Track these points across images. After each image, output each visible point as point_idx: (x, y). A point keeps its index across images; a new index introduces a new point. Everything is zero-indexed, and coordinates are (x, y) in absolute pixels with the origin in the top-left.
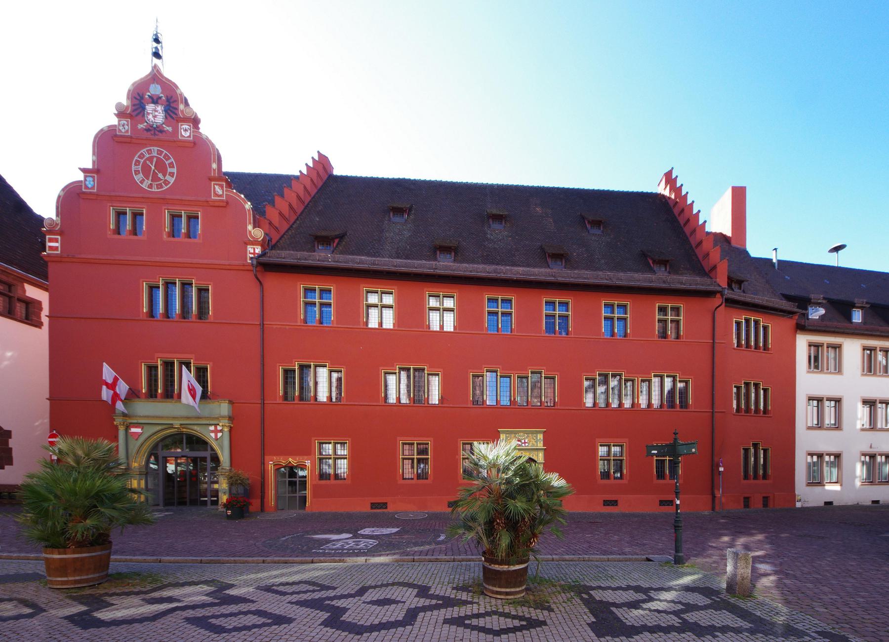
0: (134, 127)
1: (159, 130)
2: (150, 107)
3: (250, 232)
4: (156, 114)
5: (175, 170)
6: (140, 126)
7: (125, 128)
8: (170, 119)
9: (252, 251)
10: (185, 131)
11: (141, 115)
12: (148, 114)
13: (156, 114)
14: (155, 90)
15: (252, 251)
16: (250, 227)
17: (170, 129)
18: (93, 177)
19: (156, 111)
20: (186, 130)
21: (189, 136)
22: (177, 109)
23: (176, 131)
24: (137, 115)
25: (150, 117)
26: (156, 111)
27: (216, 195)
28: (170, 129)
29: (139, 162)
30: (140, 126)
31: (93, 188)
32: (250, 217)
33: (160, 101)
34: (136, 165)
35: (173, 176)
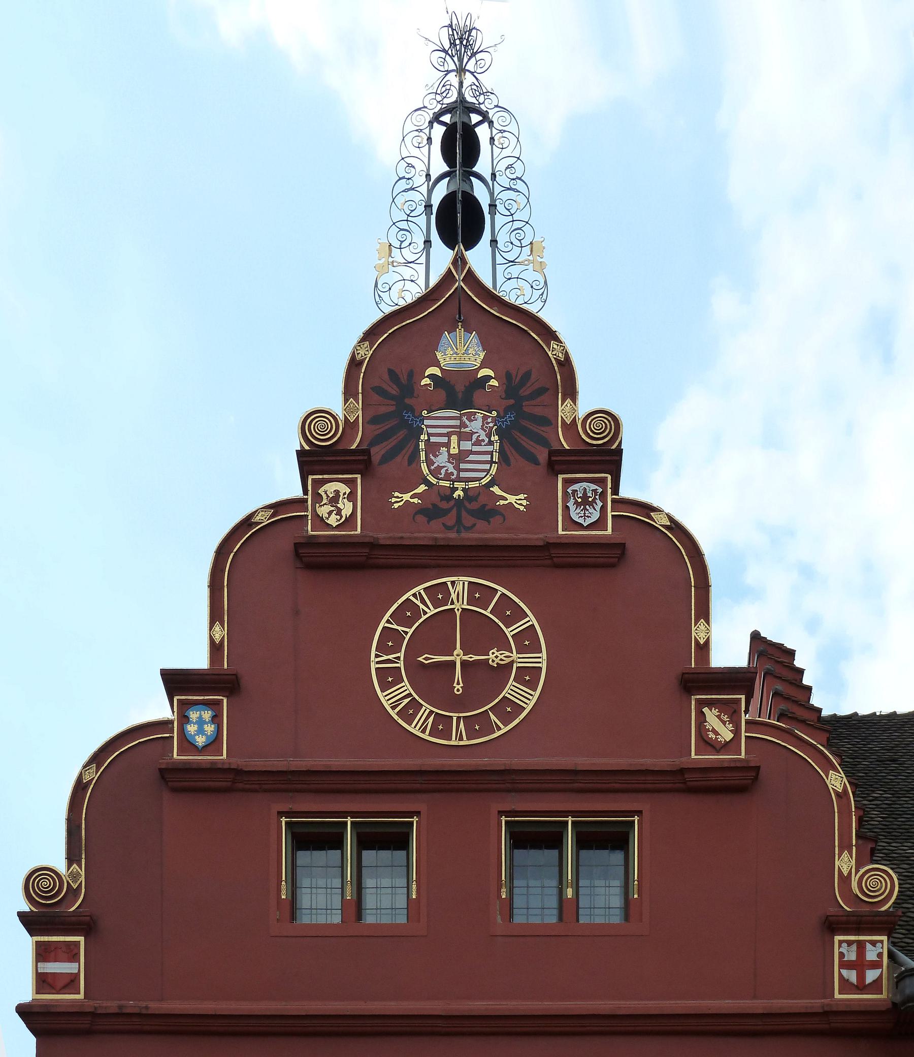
0: (375, 505)
1: (479, 505)
2: (437, 423)
3: (845, 880)
4: (461, 451)
5: (542, 660)
6: (401, 499)
7: (340, 506)
8: (517, 460)
9: (852, 956)
10: (578, 512)
11: (401, 459)
12: (433, 448)
13: (461, 451)
14: (461, 352)
15: (852, 956)
16: (845, 863)
17: (518, 501)
18: (215, 706)
19: (468, 436)
20: (585, 502)
21: (599, 524)
22: (549, 421)
23: (542, 506)
24: (385, 459)
25: (442, 459)
26: (468, 436)
27: (707, 744)
28: (518, 501)
29: (399, 636)
30: (401, 499)
31: (214, 744)
32: (844, 822)
33: (477, 396)
34: (382, 648)
35: (532, 685)
